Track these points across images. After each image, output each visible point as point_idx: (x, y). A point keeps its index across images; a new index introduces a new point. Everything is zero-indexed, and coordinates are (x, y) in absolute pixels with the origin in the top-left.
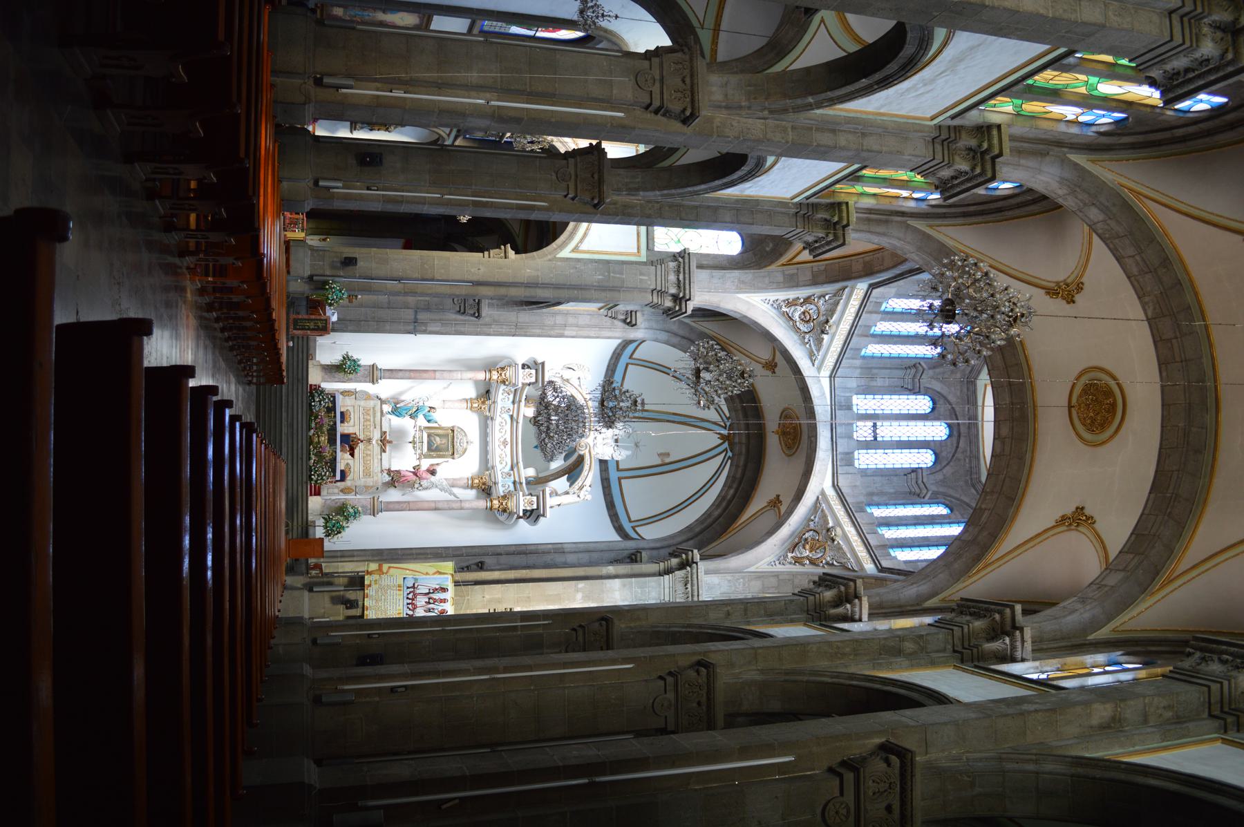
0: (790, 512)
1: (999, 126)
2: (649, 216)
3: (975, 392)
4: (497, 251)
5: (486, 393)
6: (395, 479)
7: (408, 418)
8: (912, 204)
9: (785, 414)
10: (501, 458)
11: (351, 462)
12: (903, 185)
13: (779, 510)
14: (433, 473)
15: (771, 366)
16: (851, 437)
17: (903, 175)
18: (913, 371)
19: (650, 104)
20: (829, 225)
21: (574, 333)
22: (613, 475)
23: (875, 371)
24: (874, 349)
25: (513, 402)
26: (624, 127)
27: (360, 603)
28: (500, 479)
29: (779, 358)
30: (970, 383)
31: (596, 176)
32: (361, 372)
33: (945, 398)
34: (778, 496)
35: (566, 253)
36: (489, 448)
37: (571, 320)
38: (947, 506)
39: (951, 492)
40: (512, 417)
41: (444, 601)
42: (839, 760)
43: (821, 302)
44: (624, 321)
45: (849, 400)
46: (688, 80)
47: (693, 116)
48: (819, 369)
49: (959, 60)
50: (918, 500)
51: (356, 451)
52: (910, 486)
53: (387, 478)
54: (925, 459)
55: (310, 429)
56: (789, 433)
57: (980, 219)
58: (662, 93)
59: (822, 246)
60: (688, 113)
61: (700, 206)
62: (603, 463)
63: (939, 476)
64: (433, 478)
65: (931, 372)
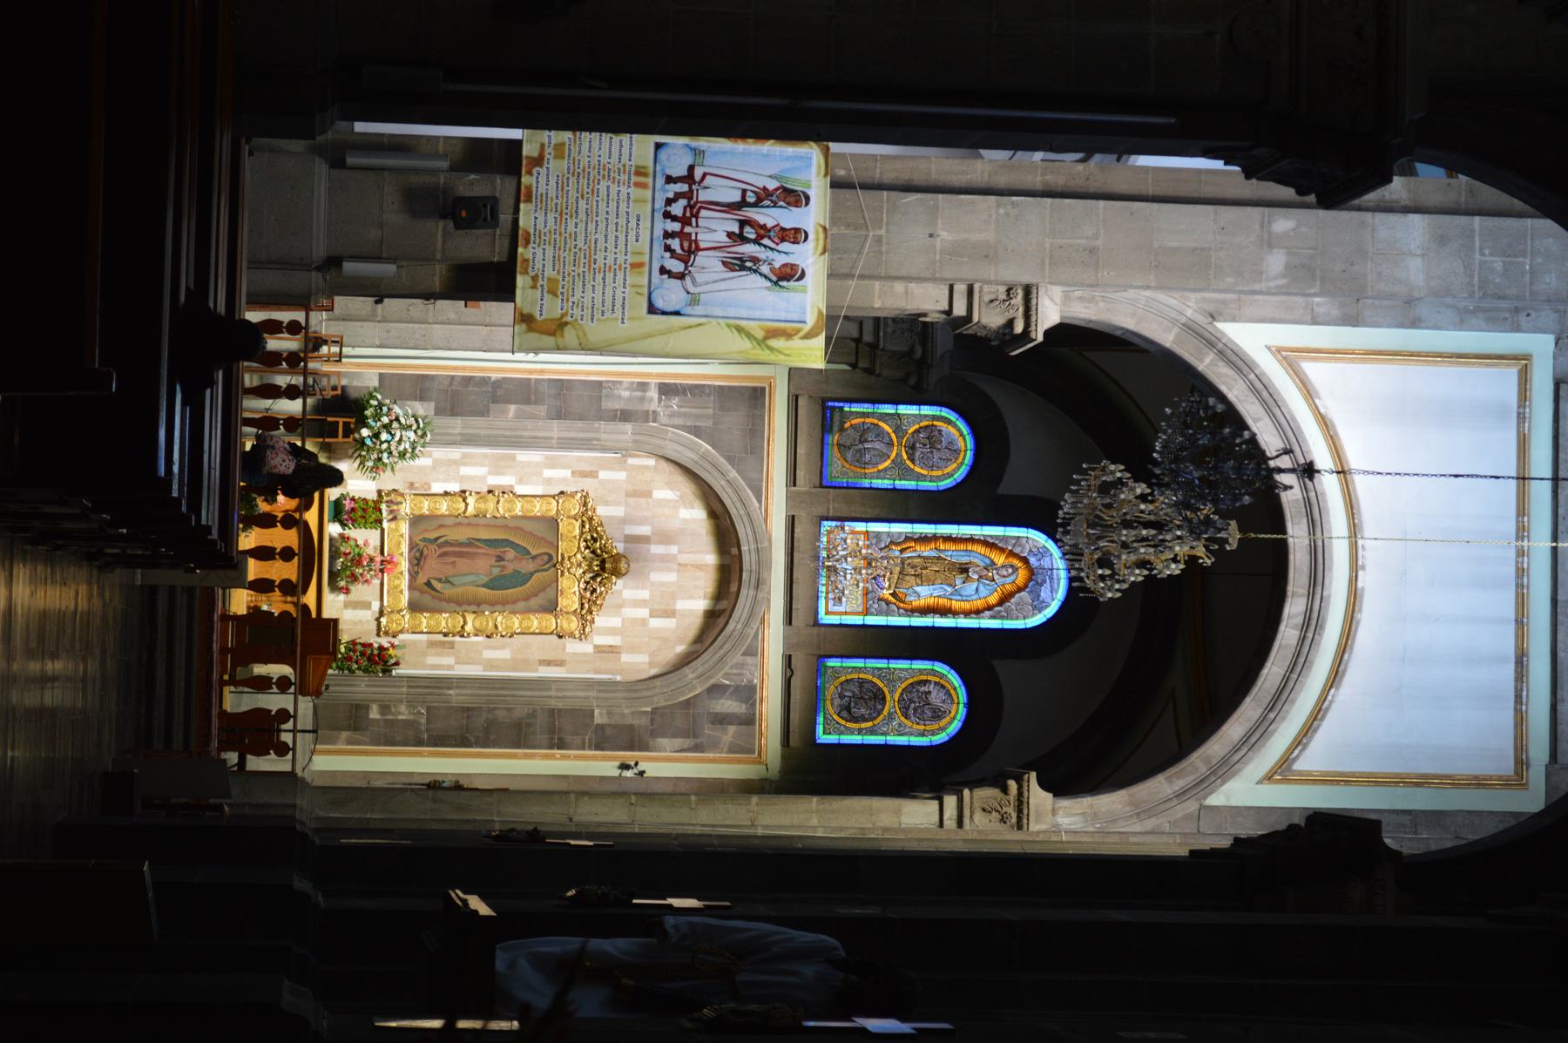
27: (505, 217)
41: (795, 235)
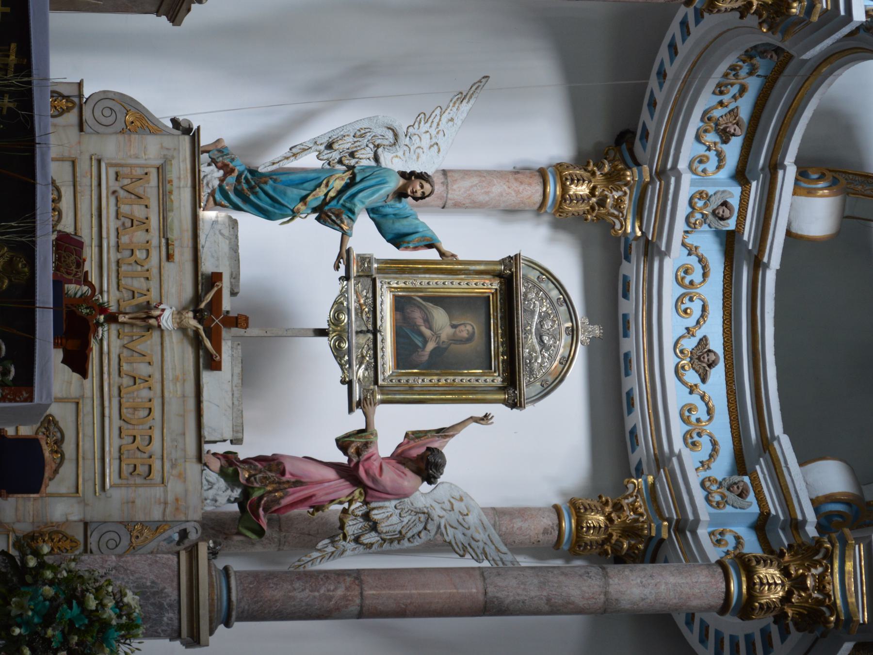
6: (263, 492)
7: (308, 224)
10: (692, 419)
25: (741, 176)
40: (730, 242)
53: (223, 499)
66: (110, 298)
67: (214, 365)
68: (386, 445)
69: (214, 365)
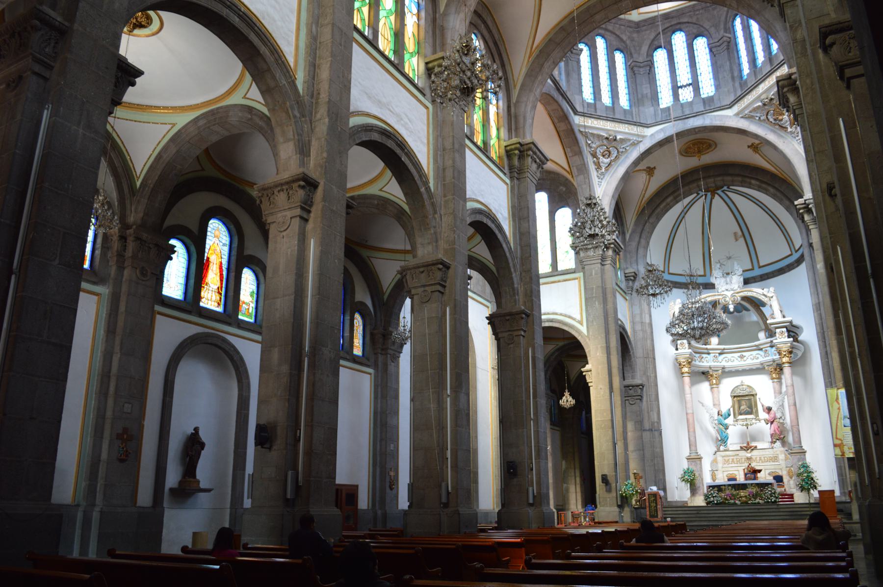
0: (756, 136)
1: (427, 63)
2: (531, 278)
3: (645, 21)
4: (587, 377)
5: (705, 375)
7: (728, 431)
8: (501, 103)
9: (686, 152)
10: (753, 358)
11: (768, 472)
12: (486, 113)
13: (758, 144)
14: (769, 409)
15: (650, 171)
16: (691, 104)
17: (478, 116)
18: (635, 69)
19: (439, 291)
20: (522, 157)
21: (647, 316)
22: (757, 272)
23: (640, 96)
24: (624, 102)
25: (709, 354)
26: (455, 306)
28: (769, 358)
29: (643, 165)
30: (638, 26)
31: (508, 318)
32: (692, 468)
33: (653, 40)
34: (749, 147)
35: (584, 329)
36: (747, 368)
37: (638, 319)
38: (734, 19)
39: (723, 18)
40: (720, 354)
42: (840, 82)
43: (594, 145)
44: (634, 281)
45: (663, 110)
46: (421, 269)
47: (442, 263)
48: (644, 137)
49: (379, 103)
50: (733, 41)
51: (758, 468)
52: (724, 51)
54: (701, 44)
55: (735, 504)
56: (699, 148)
57: (504, 56)
58: (432, 285)
59: (538, 157)
60: (441, 266)
61: (520, 245)
62: (747, 282)
63: (712, 30)
64: (774, 409)
65: (635, 56)
66: (747, 465)
67: (756, 447)
68: (766, 416)
69: (756, 447)
